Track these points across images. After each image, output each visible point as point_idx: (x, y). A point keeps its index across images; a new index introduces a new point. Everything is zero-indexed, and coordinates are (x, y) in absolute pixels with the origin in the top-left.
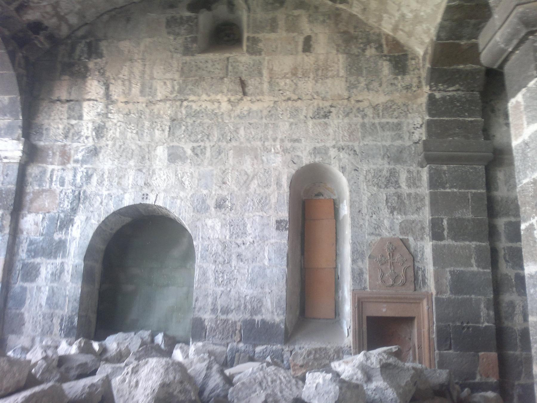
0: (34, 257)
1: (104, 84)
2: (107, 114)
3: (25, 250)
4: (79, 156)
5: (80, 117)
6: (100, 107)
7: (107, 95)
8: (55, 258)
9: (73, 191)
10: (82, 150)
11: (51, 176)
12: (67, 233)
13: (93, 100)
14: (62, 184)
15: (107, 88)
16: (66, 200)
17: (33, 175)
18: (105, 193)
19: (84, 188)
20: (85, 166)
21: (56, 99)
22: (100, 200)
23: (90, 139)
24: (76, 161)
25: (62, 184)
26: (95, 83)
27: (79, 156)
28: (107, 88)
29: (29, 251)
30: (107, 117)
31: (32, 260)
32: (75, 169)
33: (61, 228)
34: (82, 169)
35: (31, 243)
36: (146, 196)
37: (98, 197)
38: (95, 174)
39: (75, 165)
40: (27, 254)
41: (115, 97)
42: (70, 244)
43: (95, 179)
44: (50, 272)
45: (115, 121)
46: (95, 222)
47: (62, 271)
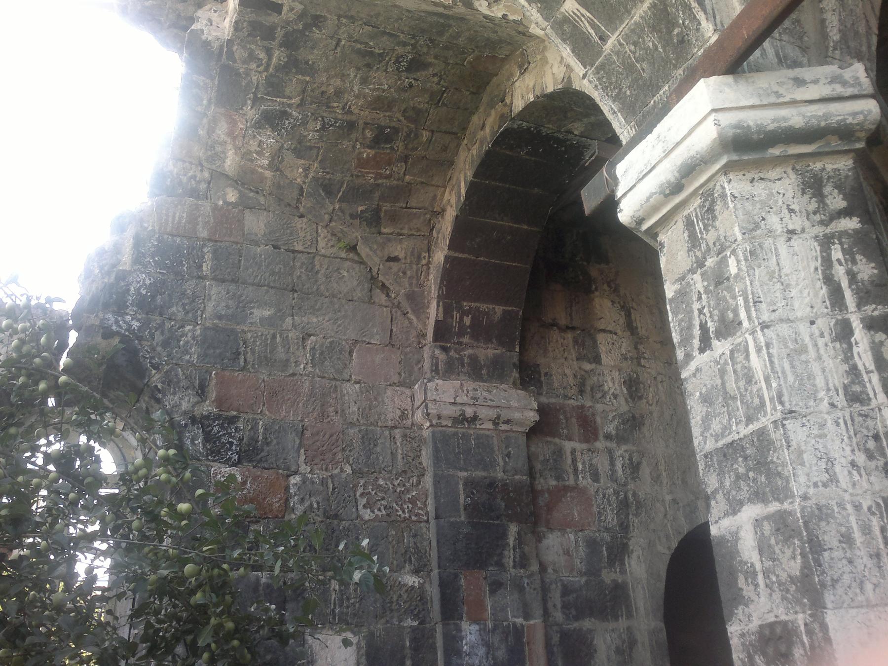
0: (577, 618)
1: (622, 307)
2: (638, 359)
3: (559, 606)
4: (611, 428)
5: (597, 360)
6: (625, 345)
7: (630, 327)
8: (617, 619)
9: (617, 493)
10: (614, 418)
11: (574, 461)
12: (623, 572)
13: (611, 332)
14: (596, 477)
15: (628, 315)
16: (608, 509)
17: (541, 458)
18: (668, 498)
19: (631, 486)
20: (624, 448)
21: (550, 321)
22: (662, 509)
23: (622, 400)
24: (608, 437)
25: (596, 477)
26: (607, 303)
27: (611, 428)
28: (628, 315)
29: (565, 607)
30: (639, 364)
31: (576, 625)
32: (610, 452)
33: (611, 562)
34: (621, 452)
35: (566, 591)
37: (658, 505)
38: (644, 463)
39: (608, 444)
40: (564, 613)
41: (642, 332)
42: (634, 591)
43: (646, 471)
44: (613, 648)
45: (654, 373)
46: (665, 550)
47: (632, 643)
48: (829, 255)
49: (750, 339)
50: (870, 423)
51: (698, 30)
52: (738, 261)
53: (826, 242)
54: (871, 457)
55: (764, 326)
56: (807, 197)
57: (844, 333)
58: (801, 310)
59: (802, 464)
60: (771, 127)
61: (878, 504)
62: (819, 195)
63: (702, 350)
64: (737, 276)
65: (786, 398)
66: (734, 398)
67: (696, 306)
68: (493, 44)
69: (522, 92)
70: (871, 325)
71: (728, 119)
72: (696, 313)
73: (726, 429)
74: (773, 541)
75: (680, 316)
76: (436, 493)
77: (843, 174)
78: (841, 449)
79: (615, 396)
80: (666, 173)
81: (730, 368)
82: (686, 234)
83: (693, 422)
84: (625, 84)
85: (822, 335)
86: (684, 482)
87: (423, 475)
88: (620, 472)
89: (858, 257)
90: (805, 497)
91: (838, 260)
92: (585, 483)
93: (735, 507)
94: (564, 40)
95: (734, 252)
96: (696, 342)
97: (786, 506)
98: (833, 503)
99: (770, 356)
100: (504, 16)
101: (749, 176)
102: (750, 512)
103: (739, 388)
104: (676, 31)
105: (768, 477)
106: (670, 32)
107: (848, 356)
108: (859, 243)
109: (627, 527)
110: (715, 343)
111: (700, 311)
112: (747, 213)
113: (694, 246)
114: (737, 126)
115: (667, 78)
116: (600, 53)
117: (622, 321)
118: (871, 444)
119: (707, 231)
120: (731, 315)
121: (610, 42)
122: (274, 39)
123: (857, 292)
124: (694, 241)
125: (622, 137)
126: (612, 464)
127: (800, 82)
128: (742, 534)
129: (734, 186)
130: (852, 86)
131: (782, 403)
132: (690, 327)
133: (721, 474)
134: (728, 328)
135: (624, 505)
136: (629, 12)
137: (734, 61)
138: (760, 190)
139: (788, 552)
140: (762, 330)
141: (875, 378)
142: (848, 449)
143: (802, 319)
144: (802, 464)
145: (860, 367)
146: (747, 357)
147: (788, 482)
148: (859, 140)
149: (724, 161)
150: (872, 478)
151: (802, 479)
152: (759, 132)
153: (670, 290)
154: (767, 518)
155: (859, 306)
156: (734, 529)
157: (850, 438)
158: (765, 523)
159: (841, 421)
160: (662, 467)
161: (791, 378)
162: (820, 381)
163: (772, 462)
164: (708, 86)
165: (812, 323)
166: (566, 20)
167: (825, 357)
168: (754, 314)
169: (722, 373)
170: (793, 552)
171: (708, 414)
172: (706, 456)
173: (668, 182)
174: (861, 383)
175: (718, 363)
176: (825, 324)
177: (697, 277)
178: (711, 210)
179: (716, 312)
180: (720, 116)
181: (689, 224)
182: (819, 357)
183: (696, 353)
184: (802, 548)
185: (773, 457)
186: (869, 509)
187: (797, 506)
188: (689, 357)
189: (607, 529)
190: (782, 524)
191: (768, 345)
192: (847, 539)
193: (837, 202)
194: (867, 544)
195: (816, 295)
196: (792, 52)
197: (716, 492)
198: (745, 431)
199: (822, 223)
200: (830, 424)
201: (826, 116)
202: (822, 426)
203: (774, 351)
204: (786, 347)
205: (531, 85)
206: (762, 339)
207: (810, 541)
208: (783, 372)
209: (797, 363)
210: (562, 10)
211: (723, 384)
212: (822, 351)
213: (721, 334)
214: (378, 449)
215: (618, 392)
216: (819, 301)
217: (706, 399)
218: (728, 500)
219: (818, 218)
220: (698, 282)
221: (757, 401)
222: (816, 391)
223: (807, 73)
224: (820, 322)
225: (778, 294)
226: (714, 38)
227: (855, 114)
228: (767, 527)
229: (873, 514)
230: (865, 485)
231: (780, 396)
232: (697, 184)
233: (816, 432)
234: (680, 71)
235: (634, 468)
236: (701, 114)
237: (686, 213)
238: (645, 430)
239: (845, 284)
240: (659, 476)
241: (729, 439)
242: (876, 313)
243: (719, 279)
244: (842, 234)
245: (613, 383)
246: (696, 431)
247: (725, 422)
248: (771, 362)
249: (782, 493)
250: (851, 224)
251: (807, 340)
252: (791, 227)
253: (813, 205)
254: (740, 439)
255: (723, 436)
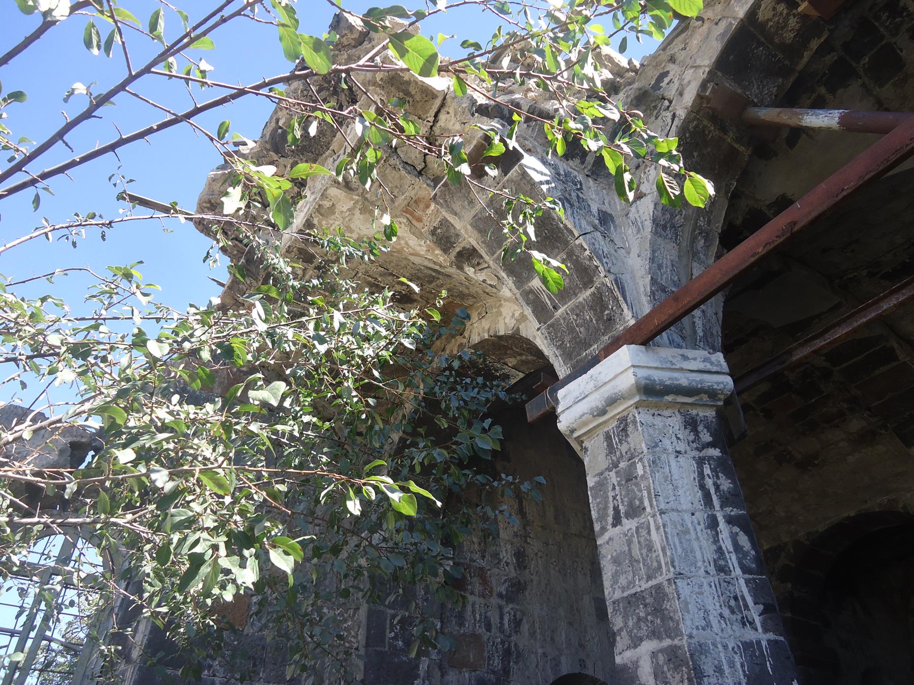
9: (503, 642)
10: (505, 581)
11: (473, 611)
14: (488, 627)
15: (521, 503)
16: (496, 655)
18: (540, 651)
20: (511, 606)
22: (535, 660)
23: (512, 567)
24: (500, 595)
25: (488, 627)
27: (502, 589)
28: (521, 503)
30: (526, 542)
32: (500, 608)
34: (508, 609)
36: (582, 663)
37: (532, 656)
38: (525, 620)
39: (500, 601)
41: (530, 517)
43: (525, 627)
48: (703, 471)
49: (651, 520)
50: (731, 587)
51: (621, 314)
52: (644, 467)
53: (700, 462)
54: (733, 612)
55: (662, 513)
56: (687, 431)
57: (713, 524)
58: (685, 505)
59: (688, 612)
60: (668, 383)
61: (738, 646)
62: (695, 431)
63: (614, 525)
64: (643, 476)
65: (676, 564)
66: (638, 561)
67: (611, 494)
68: (462, 296)
69: (479, 330)
70: (730, 521)
71: (642, 373)
72: (611, 499)
73: (631, 583)
74: (665, 669)
75: (598, 500)
76: (368, 625)
77: (710, 420)
78: (714, 606)
79: (507, 564)
80: (595, 400)
81: (635, 539)
82: (605, 444)
83: (605, 577)
84: (567, 339)
85: (699, 524)
86: (552, 639)
87: (358, 609)
88: (506, 626)
89: (720, 475)
90: (690, 636)
91: (708, 475)
92: (480, 631)
93: (636, 642)
94: (528, 304)
95: (641, 460)
96: (610, 520)
97: (676, 642)
98: (710, 642)
99: (665, 533)
100: (484, 281)
101: (652, 412)
102: (648, 646)
103: (642, 554)
104: (606, 312)
105: (662, 620)
106: (602, 312)
107: (716, 541)
108: (720, 466)
109: (509, 671)
110: (624, 521)
111: (614, 498)
112: (650, 435)
113: (611, 453)
114: (646, 379)
115: (596, 340)
116: (552, 316)
117: (516, 507)
118: (732, 603)
119: (621, 443)
120: (637, 503)
121: (560, 311)
122: (312, 263)
123: (720, 498)
124: (611, 449)
125: (559, 373)
126: (502, 618)
127: (685, 358)
128: (641, 663)
129: (642, 417)
130: (716, 365)
131: (674, 567)
132: (606, 508)
133: (626, 618)
134: (635, 511)
135: (507, 653)
136: (576, 295)
137: (644, 336)
138: (658, 421)
139: (678, 677)
140: (660, 514)
141: (734, 557)
142: (718, 604)
143: (686, 511)
144: (688, 612)
145: (724, 548)
146: (649, 533)
147: (678, 624)
148: (720, 400)
149: (637, 399)
150: (734, 627)
151: (688, 623)
152: (660, 385)
153: (591, 481)
154: (661, 651)
155: (722, 507)
156: (635, 659)
157: (718, 596)
158: (660, 655)
159: (713, 584)
160: (537, 625)
161: (679, 550)
162: (698, 554)
163: (666, 609)
164: (629, 350)
165: (693, 514)
166: (531, 291)
167: (701, 538)
168: (655, 503)
169: (629, 543)
170: (682, 677)
171: (617, 571)
172: (614, 603)
173: (597, 407)
174: (725, 559)
175: (626, 535)
176: (701, 516)
177: (613, 474)
178: (624, 430)
179: (626, 499)
180: (637, 370)
181: (608, 437)
182: (698, 539)
183: (609, 527)
184: (689, 674)
185: (667, 605)
186: (733, 649)
187: (685, 642)
188: (604, 529)
189: (493, 672)
190: (673, 655)
191: (664, 526)
192: (719, 670)
193: (706, 437)
194: (733, 675)
195: (695, 496)
196: (678, 339)
197: (621, 630)
198: (645, 586)
199: (697, 449)
200: (705, 584)
201: (701, 382)
202: (701, 586)
203: (668, 530)
204: (676, 528)
205: (487, 328)
206: (660, 521)
207: (695, 669)
208: (675, 546)
209: (684, 541)
210: (530, 285)
211: (630, 550)
212: (699, 534)
213: (628, 516)
214: (327, 582)
215: (509, 561)
216: (697, 501)
217: (616, 561)
218: (631, 636)
219: (694, 445)
220: (613, 478)
221: (655, 564)
222: (696, 562)
223: (691, 353)
224: (697, 514)
225: (670, 491)
226: (632, 322)
227: (718, 383)
228: (661, 658)
229: (736, 653)
230: (730, 632)
231: (673, 562)
232: (616, 412)
233: (697, 590)
234: (607, 338)
235: (517, 623)
236: (621, 368)
237: (606, 429)
238: (527, 593)
239: (712, 491)
240: (535, 632)
241: (633, 591)
242: (733, 513)
243: (629, 477)
244: (710, 458)
245: (507, 554)
246: (607, 584)
247: (630, 578)
248: (667, 538)
249: (673, 632)
250: (715, 452)
251: (690, 525)
252: (678, 449)
253: (692, 437)
254: (642, 591)
255: (628, 587)
